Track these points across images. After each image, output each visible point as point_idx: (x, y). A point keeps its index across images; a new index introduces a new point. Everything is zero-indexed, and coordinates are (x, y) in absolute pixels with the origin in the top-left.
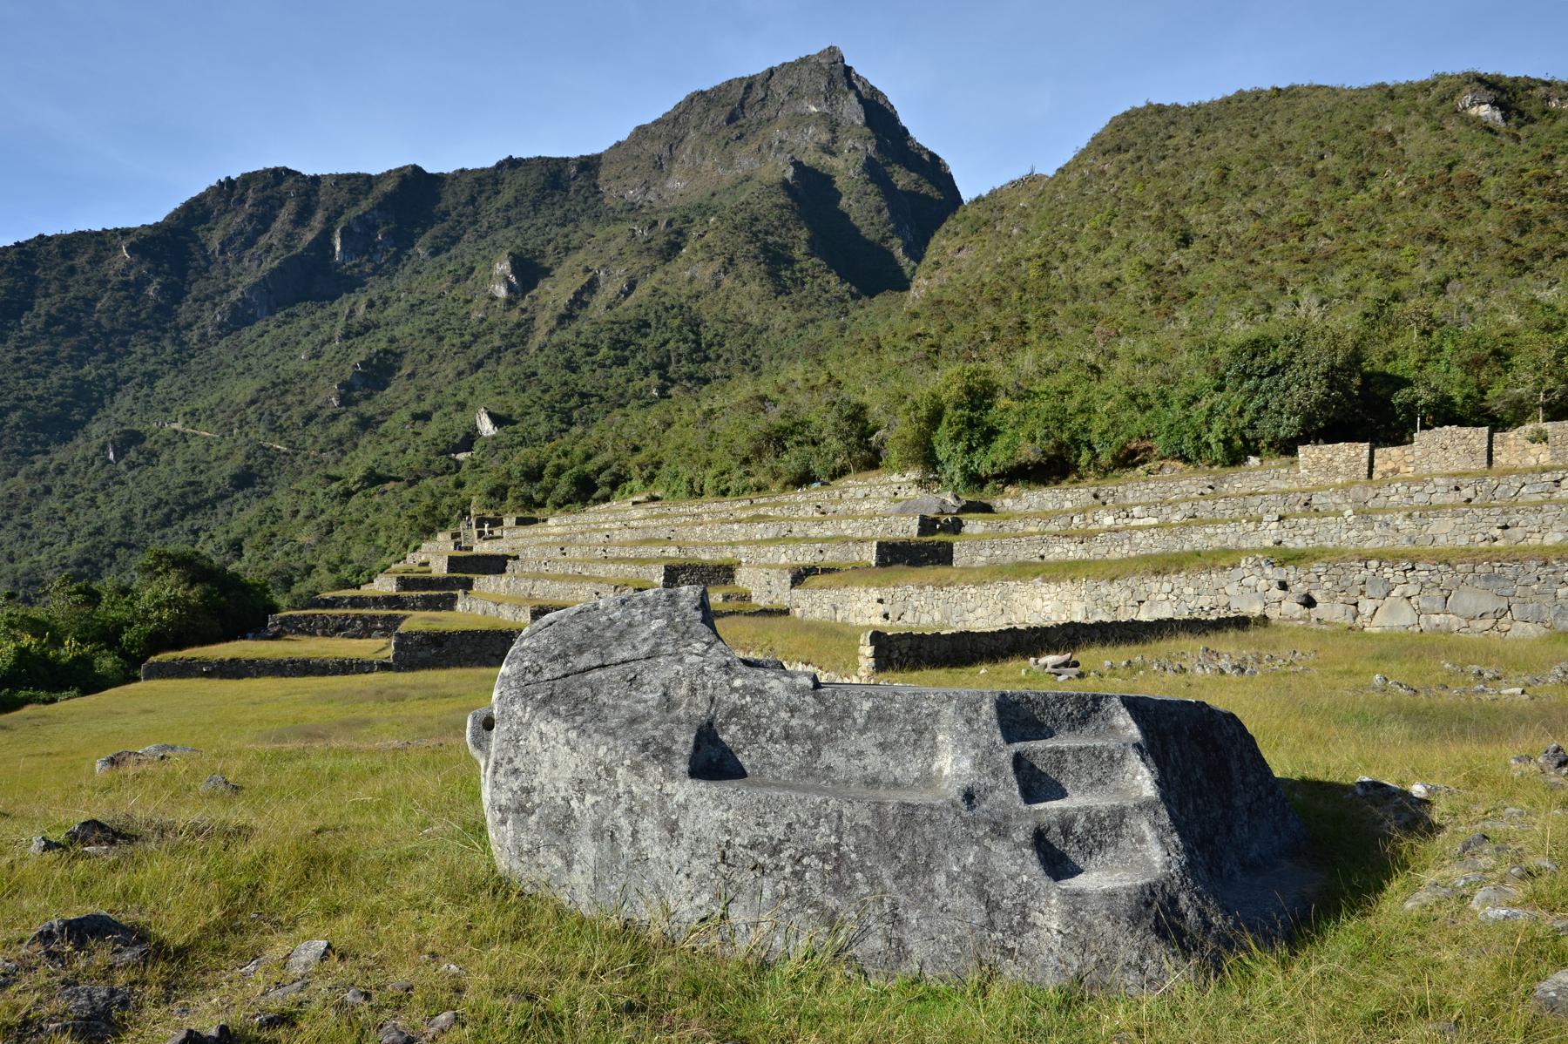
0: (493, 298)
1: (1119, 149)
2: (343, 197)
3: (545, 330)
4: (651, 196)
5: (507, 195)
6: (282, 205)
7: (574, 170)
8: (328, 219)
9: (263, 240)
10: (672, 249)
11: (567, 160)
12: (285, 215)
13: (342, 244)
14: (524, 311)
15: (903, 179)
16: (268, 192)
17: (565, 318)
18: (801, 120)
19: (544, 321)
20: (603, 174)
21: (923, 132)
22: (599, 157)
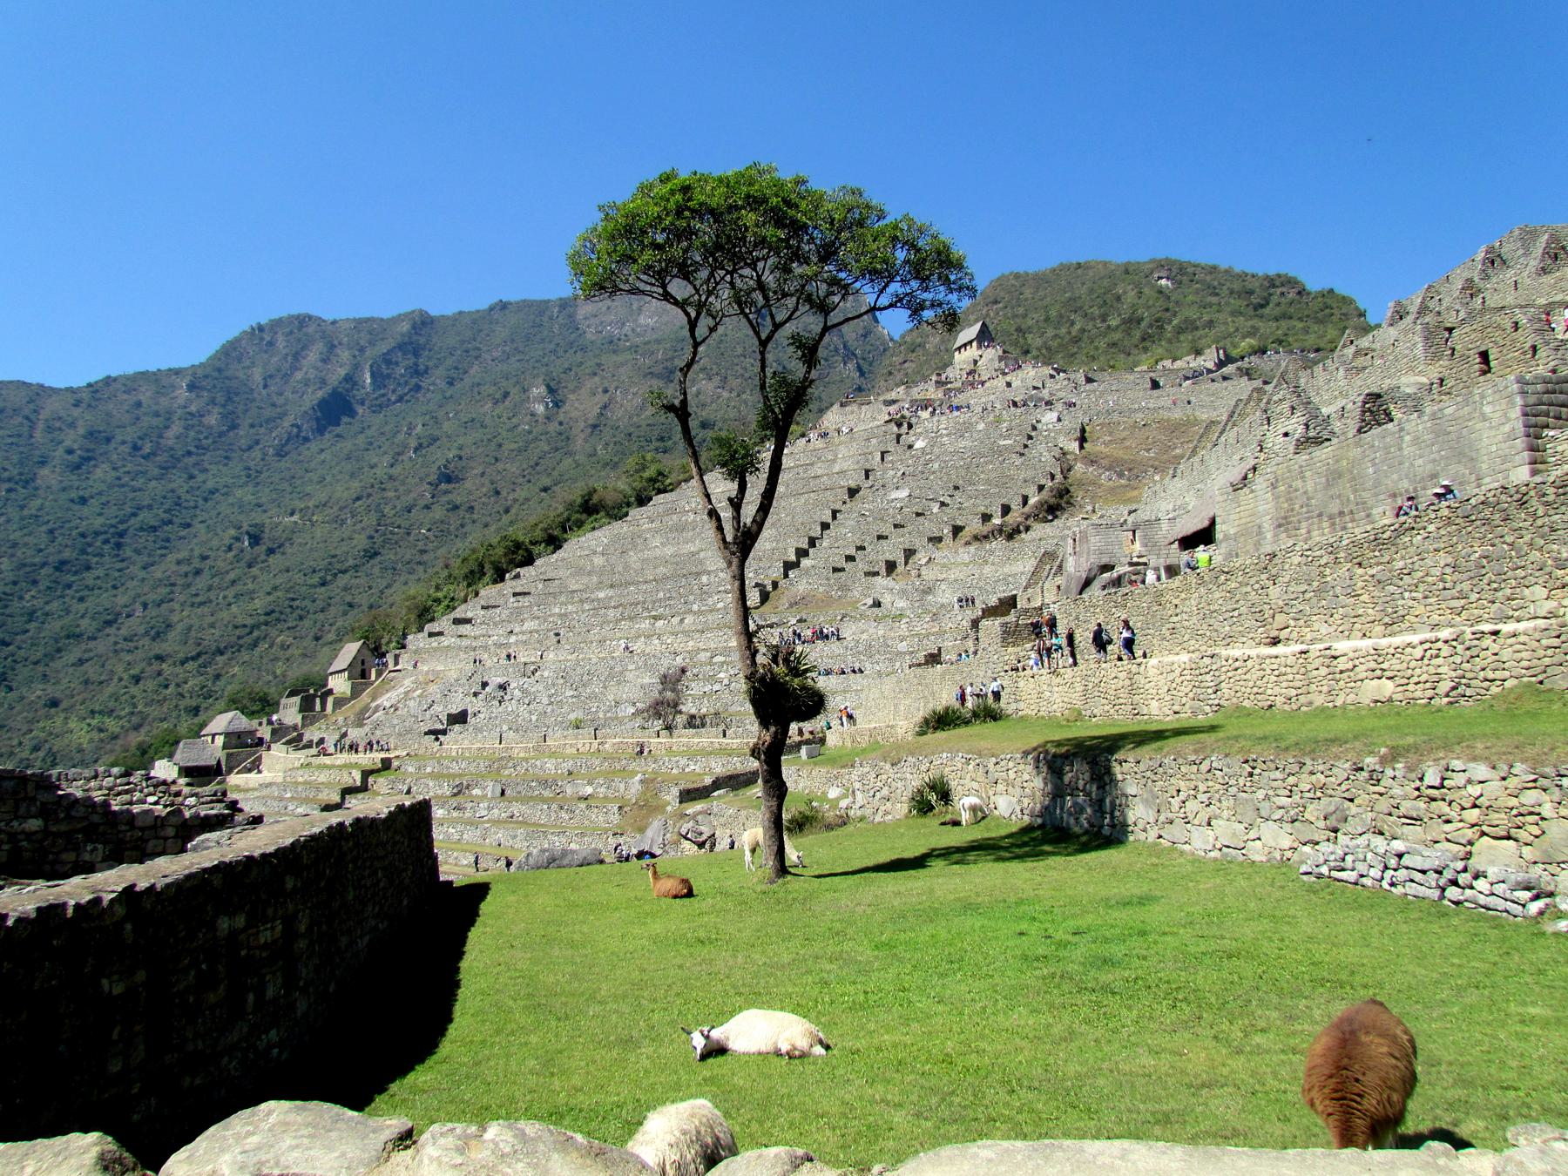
1: (996, 302)
4: (627, 329)
12: (313, 356)
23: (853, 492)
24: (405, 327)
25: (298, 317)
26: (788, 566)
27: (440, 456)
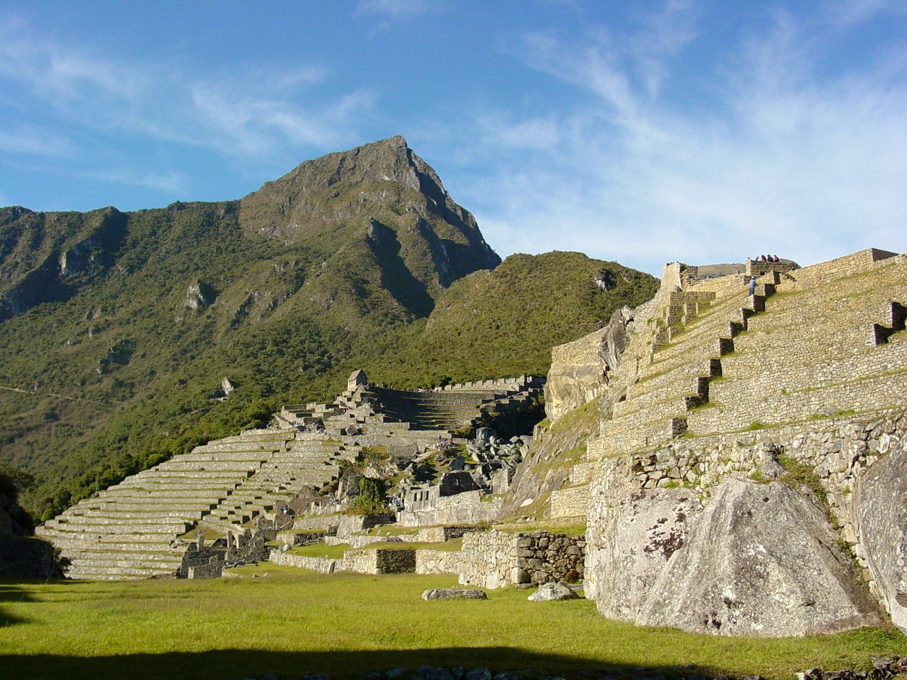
0: (188, 308)
2: (64, 229)
3: (223, 329)
4: (277, 233)
5: (177, 230)
6: (21, 235)
7: (222, 212)
8: (55, 245)
9: (9, 260)
10: (300, 279)
11: (216, 204)
12: (23, 242)
13: (67, 262)
14: (209, 317)
15: (442, 229)
16: (11, 225)
17: (236, 322)
18: (377, 186)
19: (222, 325)
20: (242, 216)
21: (457, 193)
22: (239, 202)
23: (251, 473)
24: (97, 223)
25: (14, 209)
26: (205, 513)
27: (110, 339)
